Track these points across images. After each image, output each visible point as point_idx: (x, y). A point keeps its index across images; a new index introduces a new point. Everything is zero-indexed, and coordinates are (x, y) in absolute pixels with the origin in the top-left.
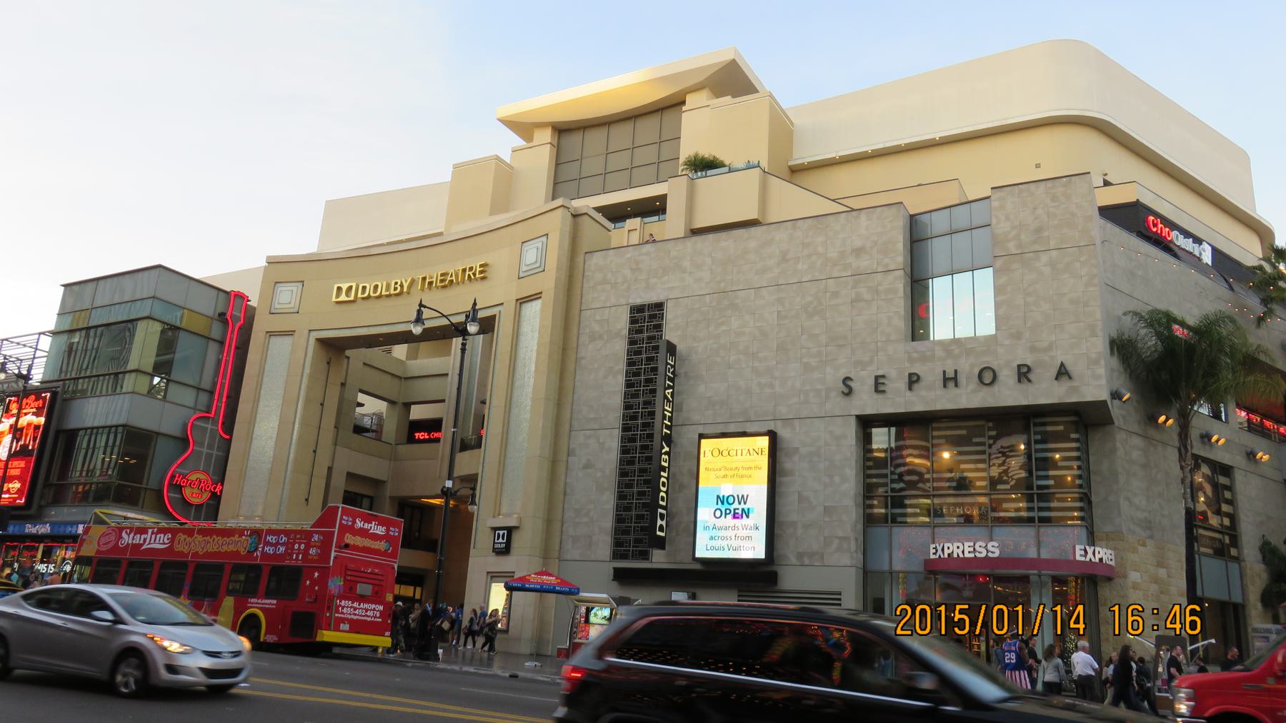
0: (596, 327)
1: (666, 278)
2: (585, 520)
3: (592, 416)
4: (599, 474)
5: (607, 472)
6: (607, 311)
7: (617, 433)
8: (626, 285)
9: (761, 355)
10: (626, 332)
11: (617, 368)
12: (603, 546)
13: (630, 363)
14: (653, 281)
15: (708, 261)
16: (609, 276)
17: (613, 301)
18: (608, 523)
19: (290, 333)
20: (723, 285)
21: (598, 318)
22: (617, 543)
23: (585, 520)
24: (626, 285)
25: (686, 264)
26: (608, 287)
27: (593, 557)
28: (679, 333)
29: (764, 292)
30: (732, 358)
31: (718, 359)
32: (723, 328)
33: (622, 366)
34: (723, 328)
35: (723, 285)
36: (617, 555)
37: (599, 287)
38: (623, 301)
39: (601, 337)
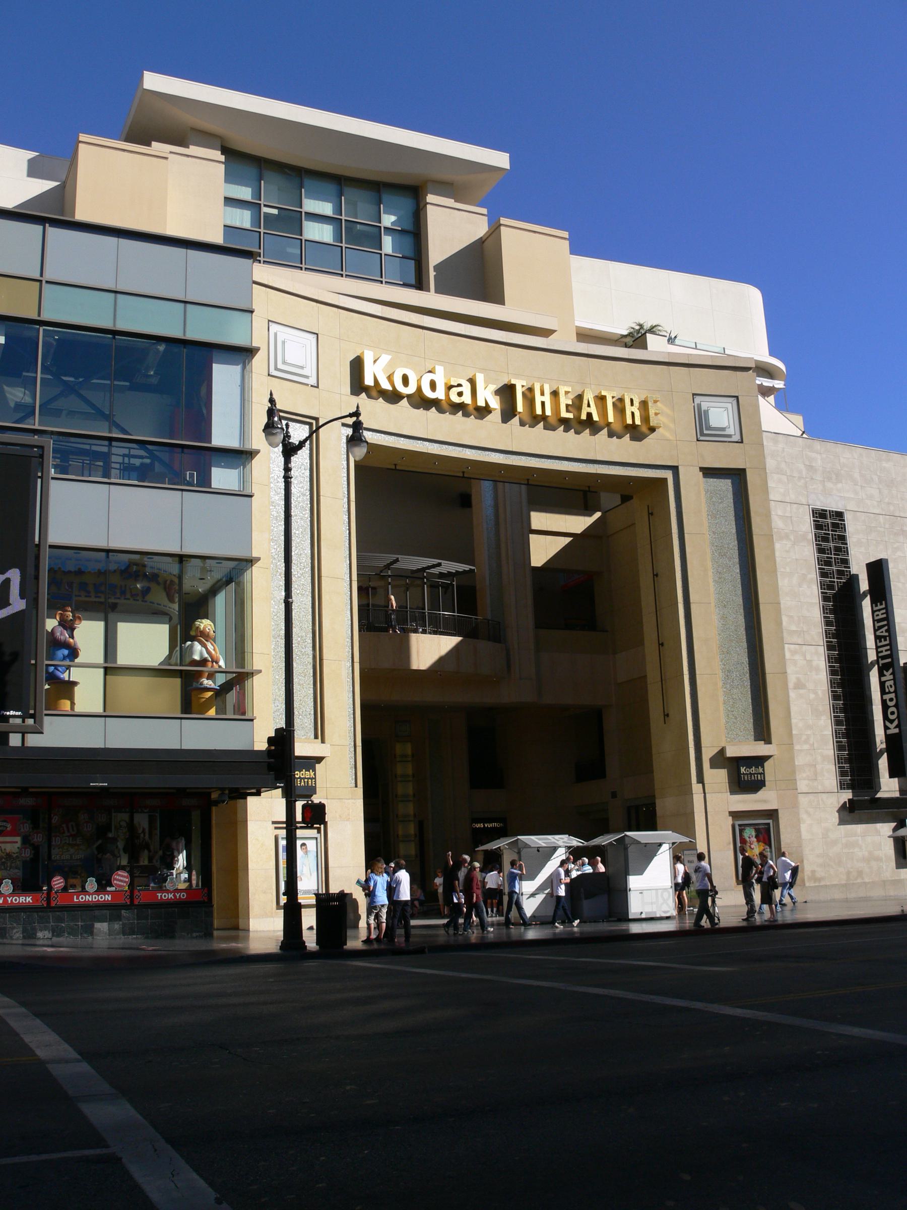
1: (840, 485)
2: (806, 747)
4: (812, 696)
5: (820, 692)
6: (788, 507)
10: (811, 536)
11: (809, 576)
14: (829, 485)
15: (876, 478)
16: (783, 465)
17: (792, 497)
21: (780, 513)
24: (803, 481)
25: (857, 475)
26: (784, 478)
27: (820, 789)
28: (863, 550)
32: (899, 554)
35: (892, 508)
39: (787, 537)
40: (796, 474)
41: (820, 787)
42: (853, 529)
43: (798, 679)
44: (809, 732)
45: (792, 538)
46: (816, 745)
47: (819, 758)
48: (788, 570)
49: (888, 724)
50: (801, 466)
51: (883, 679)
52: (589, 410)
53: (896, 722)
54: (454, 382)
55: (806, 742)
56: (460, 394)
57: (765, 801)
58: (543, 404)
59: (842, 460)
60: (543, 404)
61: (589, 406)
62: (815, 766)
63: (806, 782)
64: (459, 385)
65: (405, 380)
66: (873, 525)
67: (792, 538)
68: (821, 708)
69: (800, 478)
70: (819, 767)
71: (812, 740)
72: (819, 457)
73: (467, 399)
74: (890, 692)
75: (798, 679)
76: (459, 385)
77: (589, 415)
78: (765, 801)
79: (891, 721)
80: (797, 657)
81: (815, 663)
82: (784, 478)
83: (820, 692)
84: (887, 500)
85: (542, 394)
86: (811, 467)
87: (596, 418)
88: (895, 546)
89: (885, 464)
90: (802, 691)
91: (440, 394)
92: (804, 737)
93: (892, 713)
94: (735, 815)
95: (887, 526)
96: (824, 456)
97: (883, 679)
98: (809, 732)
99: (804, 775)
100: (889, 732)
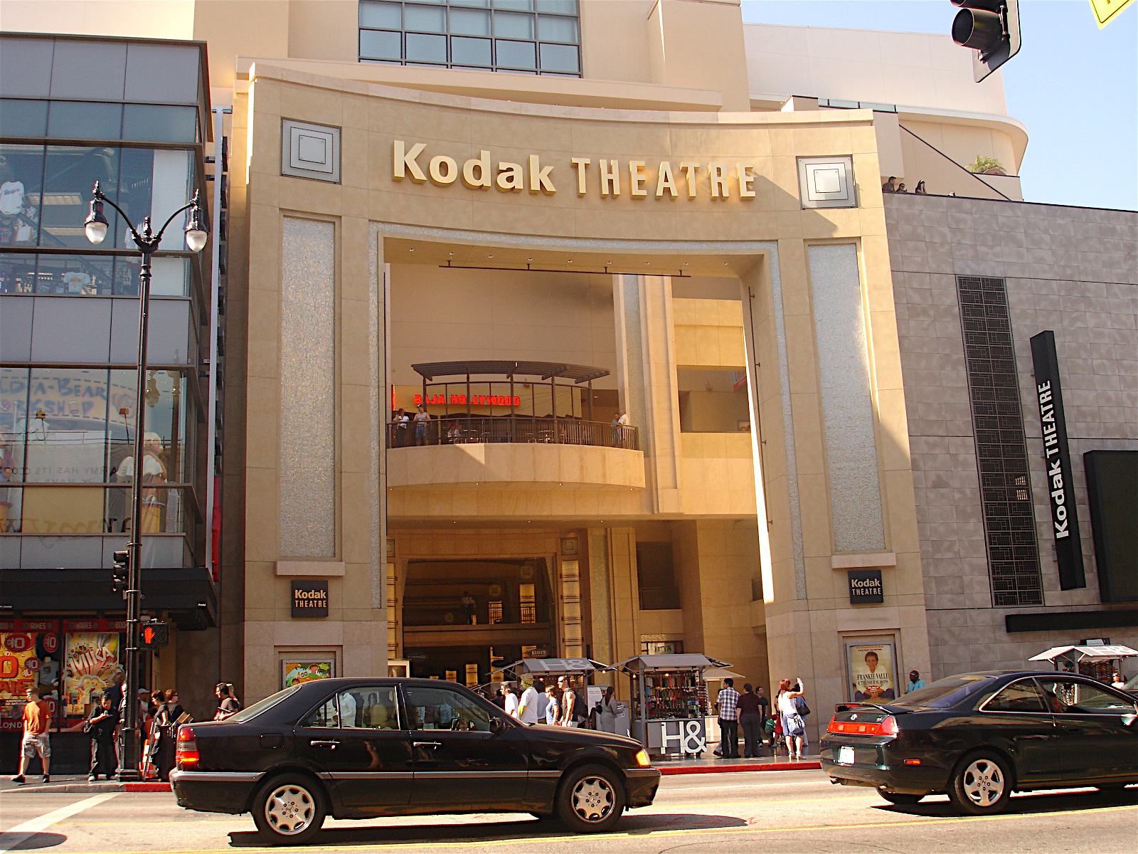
0: (916, 298)
1: (997, 249)
2: (949, 555)
3: (933, 417)
4: (957, 496)
5: (968, 491)
6: (927, 278)
7: (971, 441)
8: (947, 247)
9: (1125, 362)
10: (956, 310)
11: (955, 357)
12: (981, 590)
13: (972, 352)
14: (983, 249)
15: (1047, 238)
16: (920, 230)
18: (981, 559)
19: (333, 220)
20: (1069, 271)
21: (915, 286)
22: (998, 585)
23: (949, 555)
24: (947, 247)
25: (1021, 236)
26: (922, 245)
27: (968, 604)
28: (1028, 322)
29: (1115, 288)
30: (1096, 362)
31: (1080, 362)
32: (1079, 324)
33: (960, 355)
34: (1079, 324)
36: (999, 600)
37: (910, 244)
38: (948, 270)
39: (925, 312)
40: (937, 239)
41: (967, 602)
42: (1014, 297)
43: (939, 477)
44: (954, 538)
45: (932, 313)
46: (962, 553)
47: (967, 568)
48: (925, 350)
49: (1057, 526)
50: (946, 230)
51: (1051, 473)
52: (667, 185)
53: (1065, 524)
54: (503, 166)
55: (949, 549)
56: (510, 179)
57: (884, 619)
58: (611, 182)
59: (1001, 219)
60: (611, 182)
61: (666, 180)
62: (961, 577)
63: (949, 596)
64: (510, 170)
65: (444, 167)
66: (1043, 292)
67: (932, 313)
68: (969, 510)
69: (942, 245)
70: (966, 579)
71: (956, 548)
72: (968, 217)
73: (518, 183)
74: (1058, 489)
75: (939, 477)
76: (510, 170)
77: (667, 190)
78: (884, 619)
79: (1061, 523)
80: (937, 451)
81: (961, 458)
82: (922, 245)
83: (968, 491)
84: (1062, 263)
85: (610, 172)
86: (960, 230)
87: (674, 193)
88: (1074, 316)
89: (1060, 221)
90: (942, 491)
91: (486, 180)
92: (946, 545)
93: (1062, 513)
94: (845, 635)
95: (1063, 293)
96: (977, 216)
97: (1051, 473)
98: (954, 538)
99: (946, 588)
100: (1059, 536)
